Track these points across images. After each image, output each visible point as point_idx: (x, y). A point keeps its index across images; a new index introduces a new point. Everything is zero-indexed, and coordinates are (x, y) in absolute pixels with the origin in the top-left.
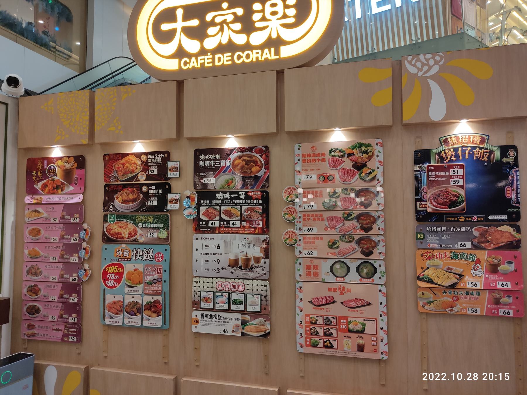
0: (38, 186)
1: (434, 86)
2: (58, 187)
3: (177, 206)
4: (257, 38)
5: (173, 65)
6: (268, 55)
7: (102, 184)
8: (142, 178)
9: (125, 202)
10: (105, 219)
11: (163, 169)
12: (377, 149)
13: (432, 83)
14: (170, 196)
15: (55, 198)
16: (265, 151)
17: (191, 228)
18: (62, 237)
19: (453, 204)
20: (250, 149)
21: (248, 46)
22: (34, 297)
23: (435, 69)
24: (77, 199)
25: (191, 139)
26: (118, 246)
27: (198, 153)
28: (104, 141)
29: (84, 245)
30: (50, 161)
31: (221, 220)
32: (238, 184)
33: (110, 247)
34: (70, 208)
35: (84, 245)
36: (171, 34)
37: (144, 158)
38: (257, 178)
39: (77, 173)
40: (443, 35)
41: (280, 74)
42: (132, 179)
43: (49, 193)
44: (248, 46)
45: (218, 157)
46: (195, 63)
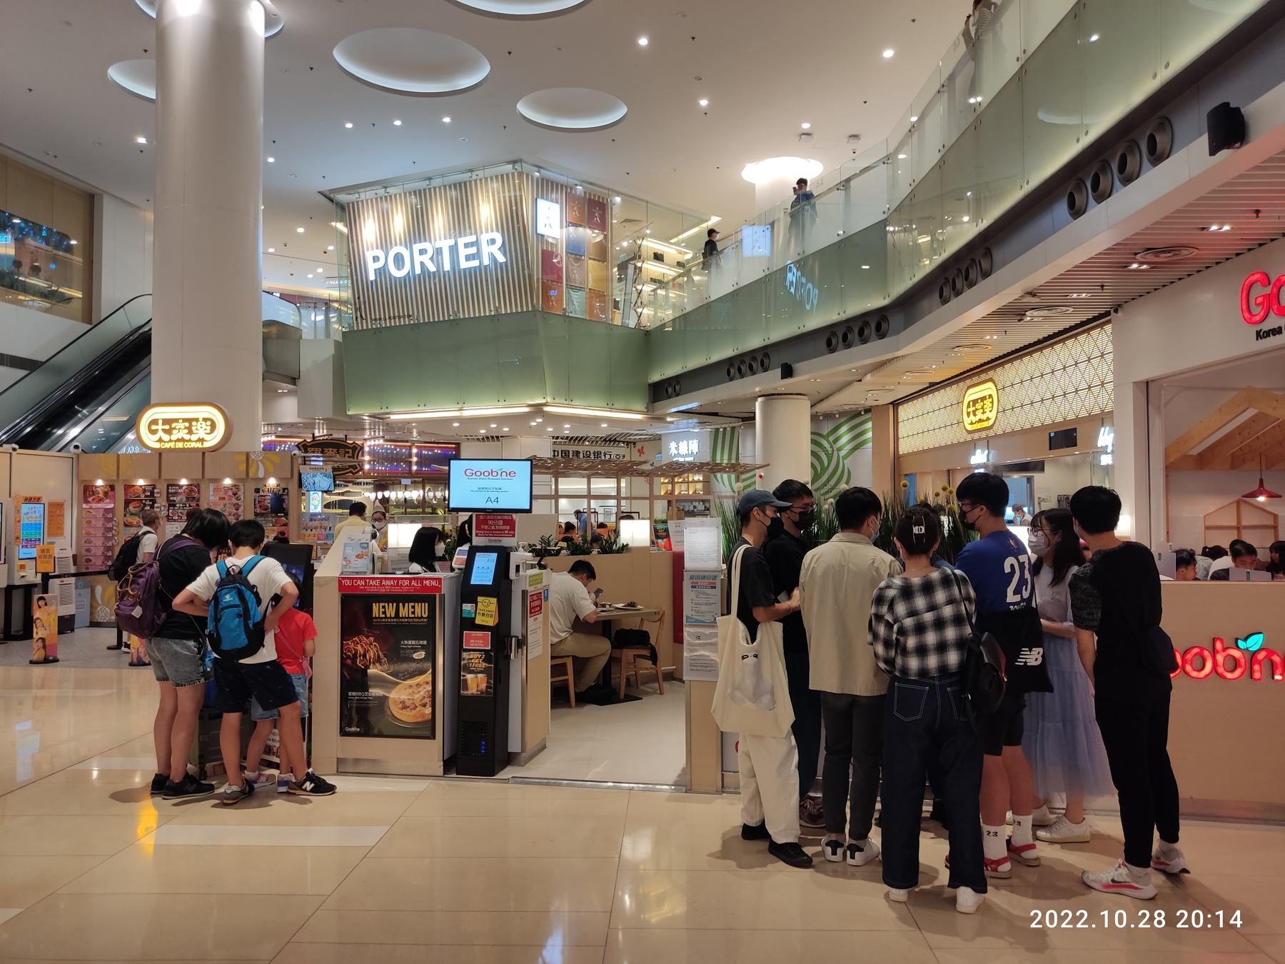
0: (90, 499)
1: (261, 465)
2: (100, 500)
3: (159, 510)
4: (194, 437)
5: (157, 445)
6: (199, 445)
7: (124, 499)
8: (143, 497)
9: (134, 507)
10: (125, 516)
11: (152, 493)
12: (242, 487)
13: (259, 462)
14: (156, 505)
15: (99, 505)
16: (198, 486)
17: (166, 519)
18: (104, 524)
19: (266, 509)
20: (191, 485)
21: (190, 440)
22: (89, 554)
23: (261, 458)
24: (111, 506)
25: (166, 480)
26: (131, 528)
27: (168, 486)
28: (124, 478)
29: (115, 528)
30: (96, 487)
31: (179, 516)
32: (184, 500)
33: (127, 528)
34: (107, 511)
35: (115, 528)
36: (157, 430)
37: (143, 487)
38: (194, 498)
39: (111, 493)
40: (520, 311)
41: (204, 453)
42: (137, 497)
43: (96, 503)
44: (190, 440)
45: (177, 488)
46: (167, 446)
